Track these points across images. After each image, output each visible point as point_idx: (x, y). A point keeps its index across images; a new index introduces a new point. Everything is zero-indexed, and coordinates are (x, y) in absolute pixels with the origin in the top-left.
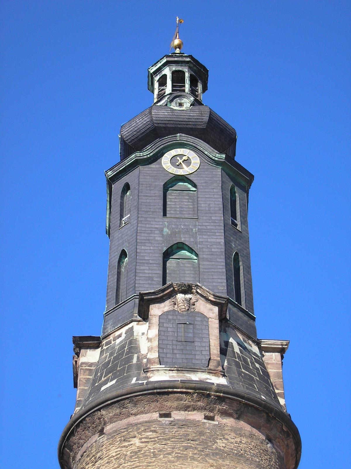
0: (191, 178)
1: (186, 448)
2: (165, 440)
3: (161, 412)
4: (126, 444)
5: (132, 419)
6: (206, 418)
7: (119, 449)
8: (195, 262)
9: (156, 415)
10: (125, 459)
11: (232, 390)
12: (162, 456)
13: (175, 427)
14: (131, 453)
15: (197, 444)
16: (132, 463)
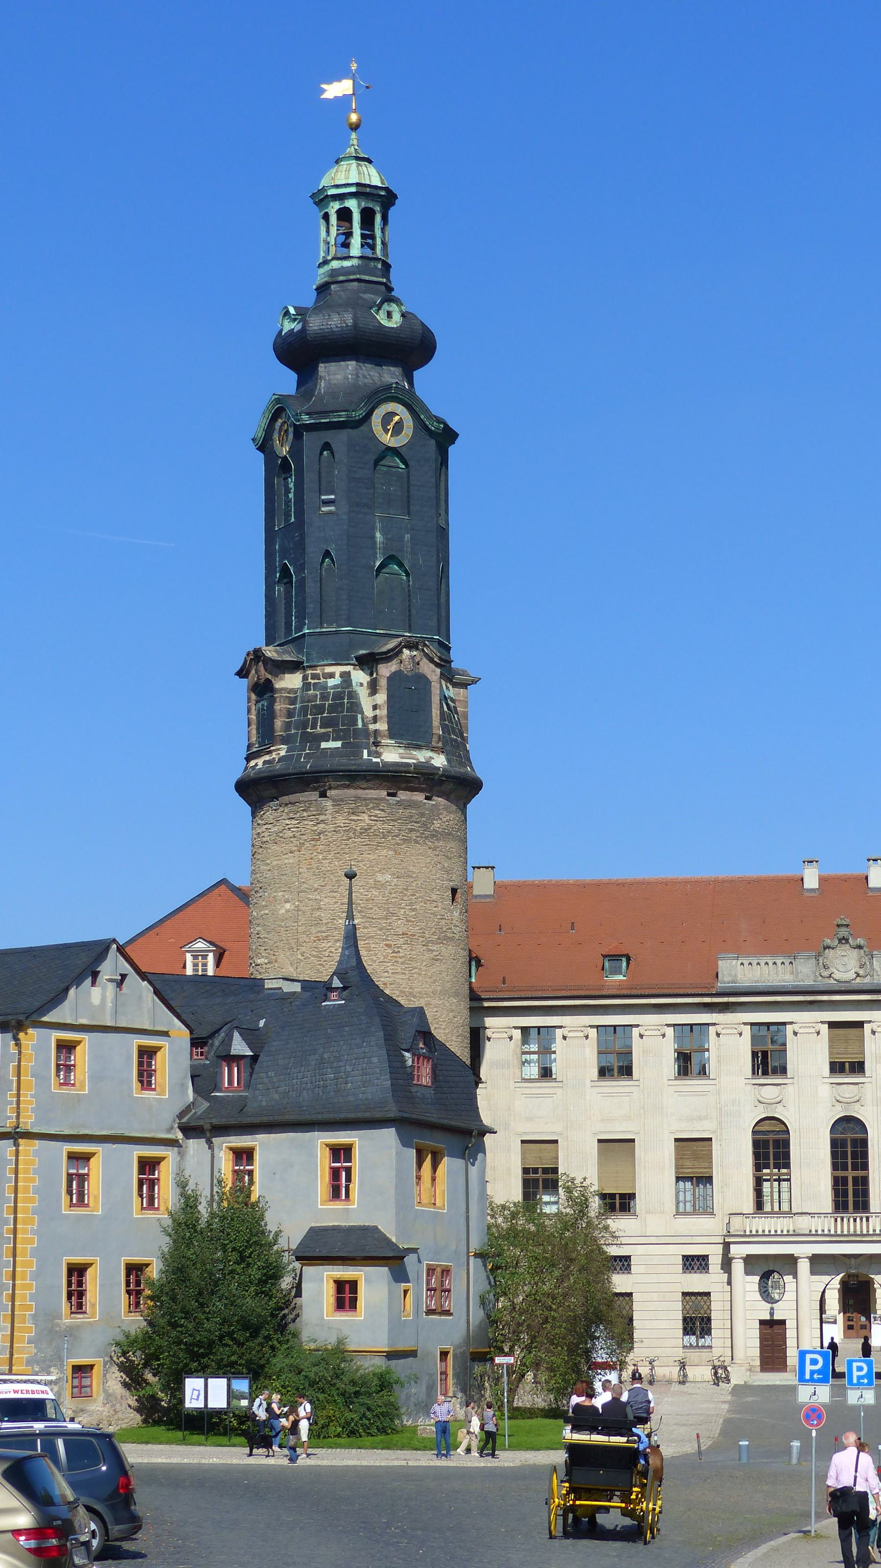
0: (403, 452)
1: (411, 830)
2: (393, 820)
3: (389, 791)
4: (355, 818)
5: (360, 792)
6: (427, 798)
7: (347, 821)
8: (403, 580)
9: (384, 793)
10: (354, 833)
11: (453, 773)
12: (390, 838)
13: (401, 807)
14: (361, 829)
15: (420, 827)
16: (363, 840)
